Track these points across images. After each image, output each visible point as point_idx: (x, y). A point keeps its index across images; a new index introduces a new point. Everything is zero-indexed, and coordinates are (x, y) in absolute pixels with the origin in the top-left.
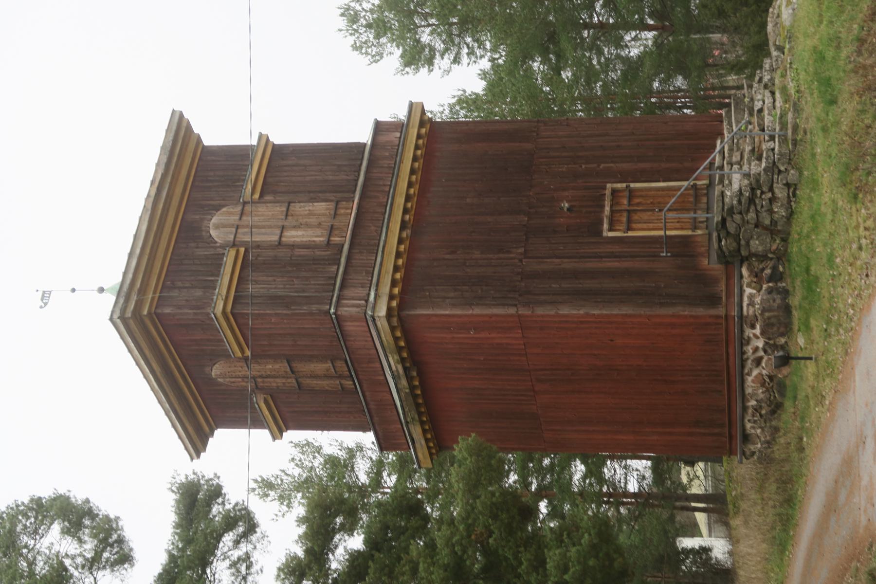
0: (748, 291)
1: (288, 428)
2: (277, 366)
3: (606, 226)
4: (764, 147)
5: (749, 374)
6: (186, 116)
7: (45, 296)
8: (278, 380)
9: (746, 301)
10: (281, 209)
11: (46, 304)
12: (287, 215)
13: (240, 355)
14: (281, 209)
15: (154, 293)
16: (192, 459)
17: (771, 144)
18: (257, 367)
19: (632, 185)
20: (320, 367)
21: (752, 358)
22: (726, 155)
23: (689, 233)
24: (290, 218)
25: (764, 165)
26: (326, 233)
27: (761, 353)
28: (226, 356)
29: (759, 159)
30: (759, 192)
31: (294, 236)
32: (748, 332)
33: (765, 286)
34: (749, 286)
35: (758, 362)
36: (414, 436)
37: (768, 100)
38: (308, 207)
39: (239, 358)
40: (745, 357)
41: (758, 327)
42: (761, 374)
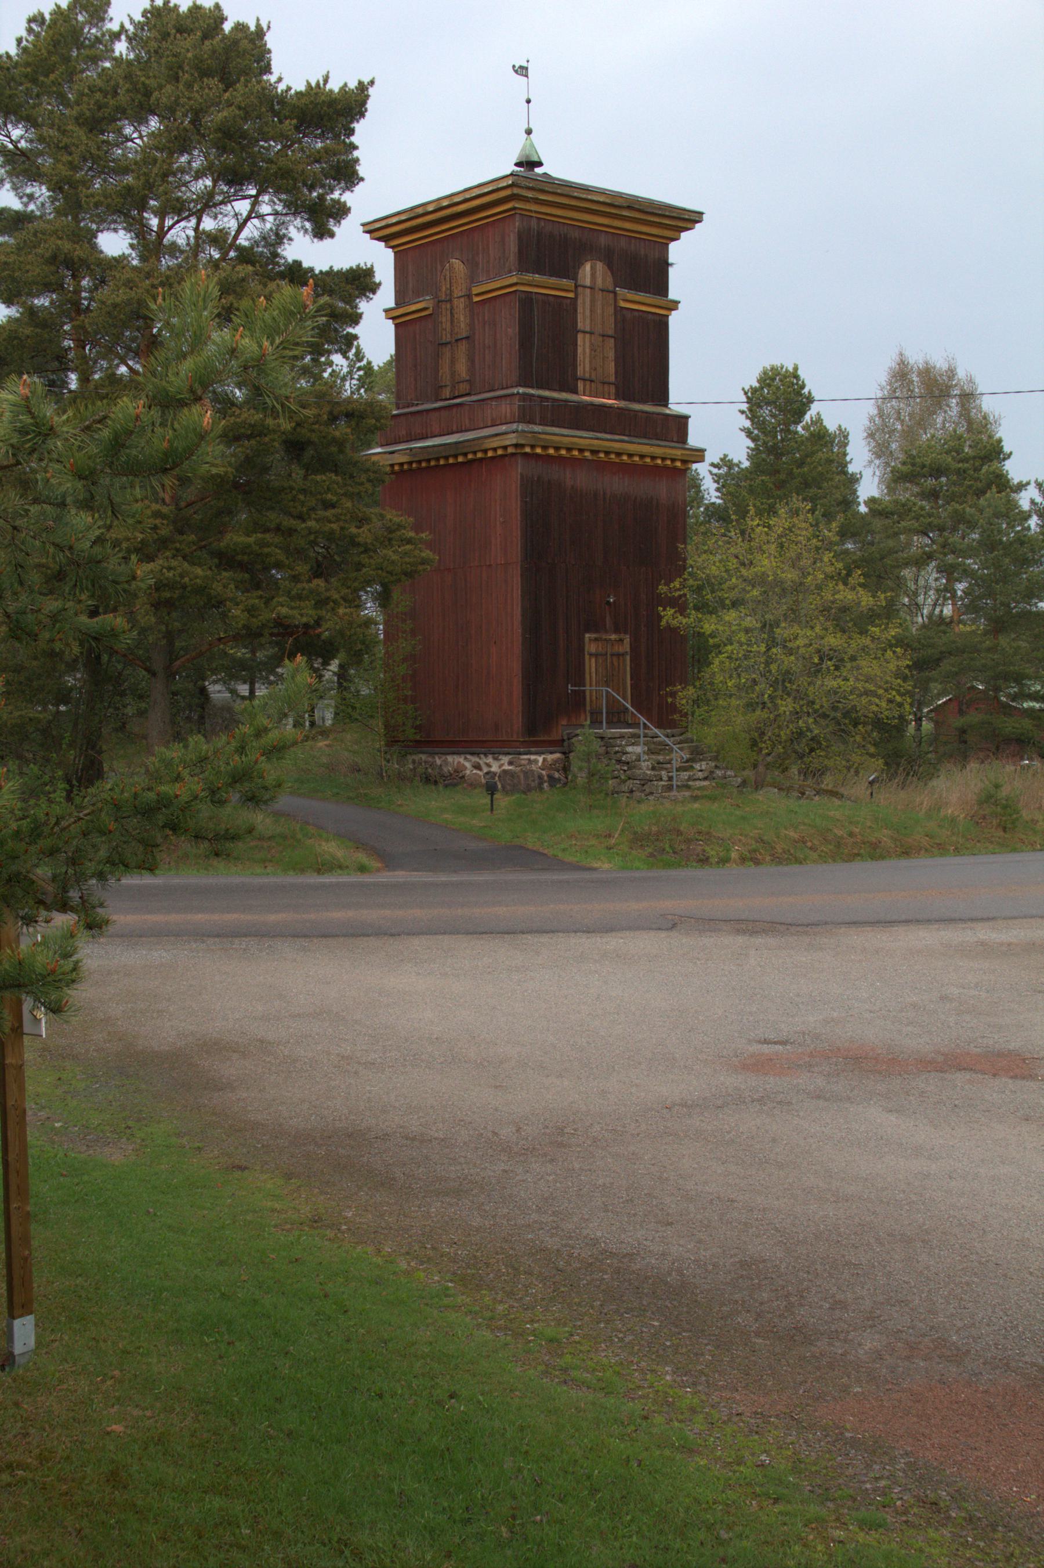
0: (540, 759)
1: (397, 326)
2: (463, 325)
3: (594, 636)
4: (663, 773)
5: (466, 758)
6: (697, 226)
7: (522, 71)
8: (449, 324)
9: (533, 757)
10: (611, 332)
11: (516, 72)
12: (603, 336)
13: (474, 292)
14: (611, 332)
15: (536, 212)
16: (363, 225)
17: (665, 778)
18: (462, 306)
19: (628, 658)
20: (462, 368)
21: (481, 762)
22: (655, 740)
23: (588, 708)
24: (601, 339)
25: (649, 772)
26: (587, 376)
27: (485, 770)
28: (472, 279)
29: (653, 768)
30: (625, 768)
31: (583, 345)
32: (505, 759)
33: (544, 772)
34: (544, 760)
35: (478, 767)
36: (396, 455)
37: (700, 775)
38: (611, 354)
39: (470, 290)
40: (482, 756)
41: (510, 768)
42: (466, 768)
